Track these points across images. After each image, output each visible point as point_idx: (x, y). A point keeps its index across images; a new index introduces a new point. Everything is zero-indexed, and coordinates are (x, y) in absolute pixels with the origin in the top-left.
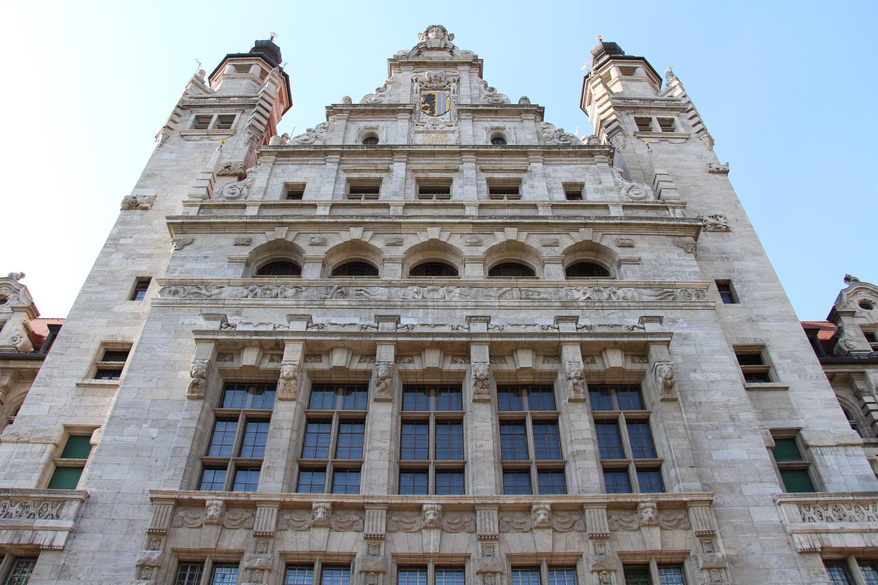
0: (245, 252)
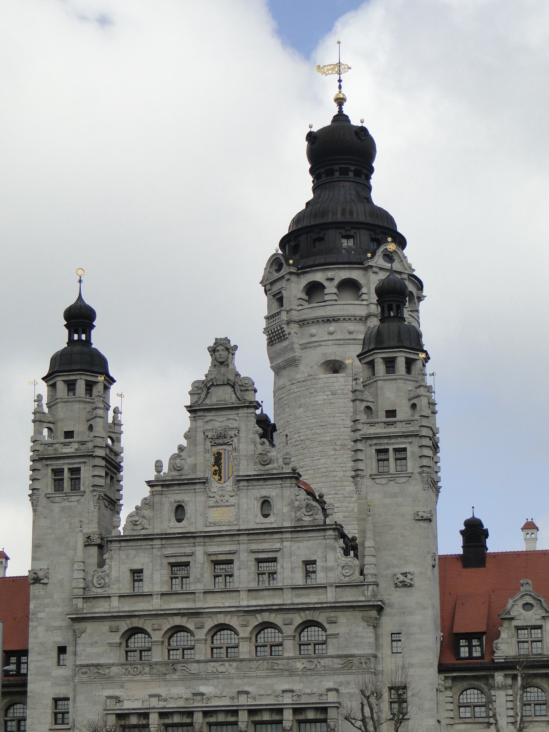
0: (116, 638)
